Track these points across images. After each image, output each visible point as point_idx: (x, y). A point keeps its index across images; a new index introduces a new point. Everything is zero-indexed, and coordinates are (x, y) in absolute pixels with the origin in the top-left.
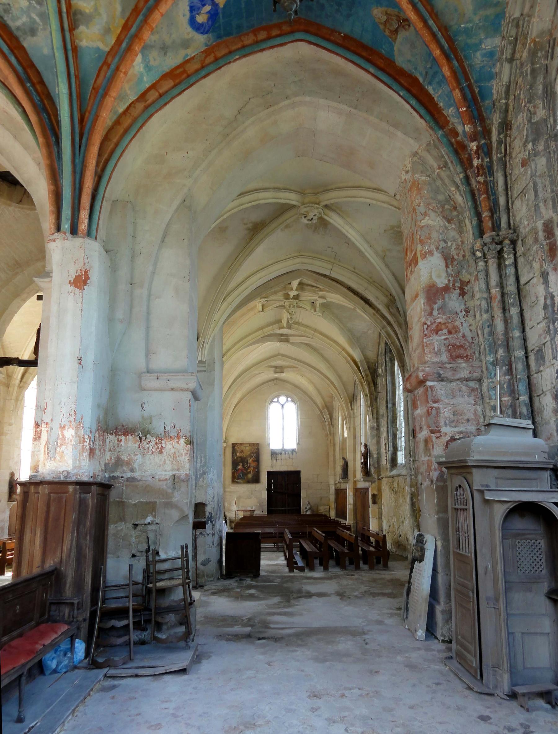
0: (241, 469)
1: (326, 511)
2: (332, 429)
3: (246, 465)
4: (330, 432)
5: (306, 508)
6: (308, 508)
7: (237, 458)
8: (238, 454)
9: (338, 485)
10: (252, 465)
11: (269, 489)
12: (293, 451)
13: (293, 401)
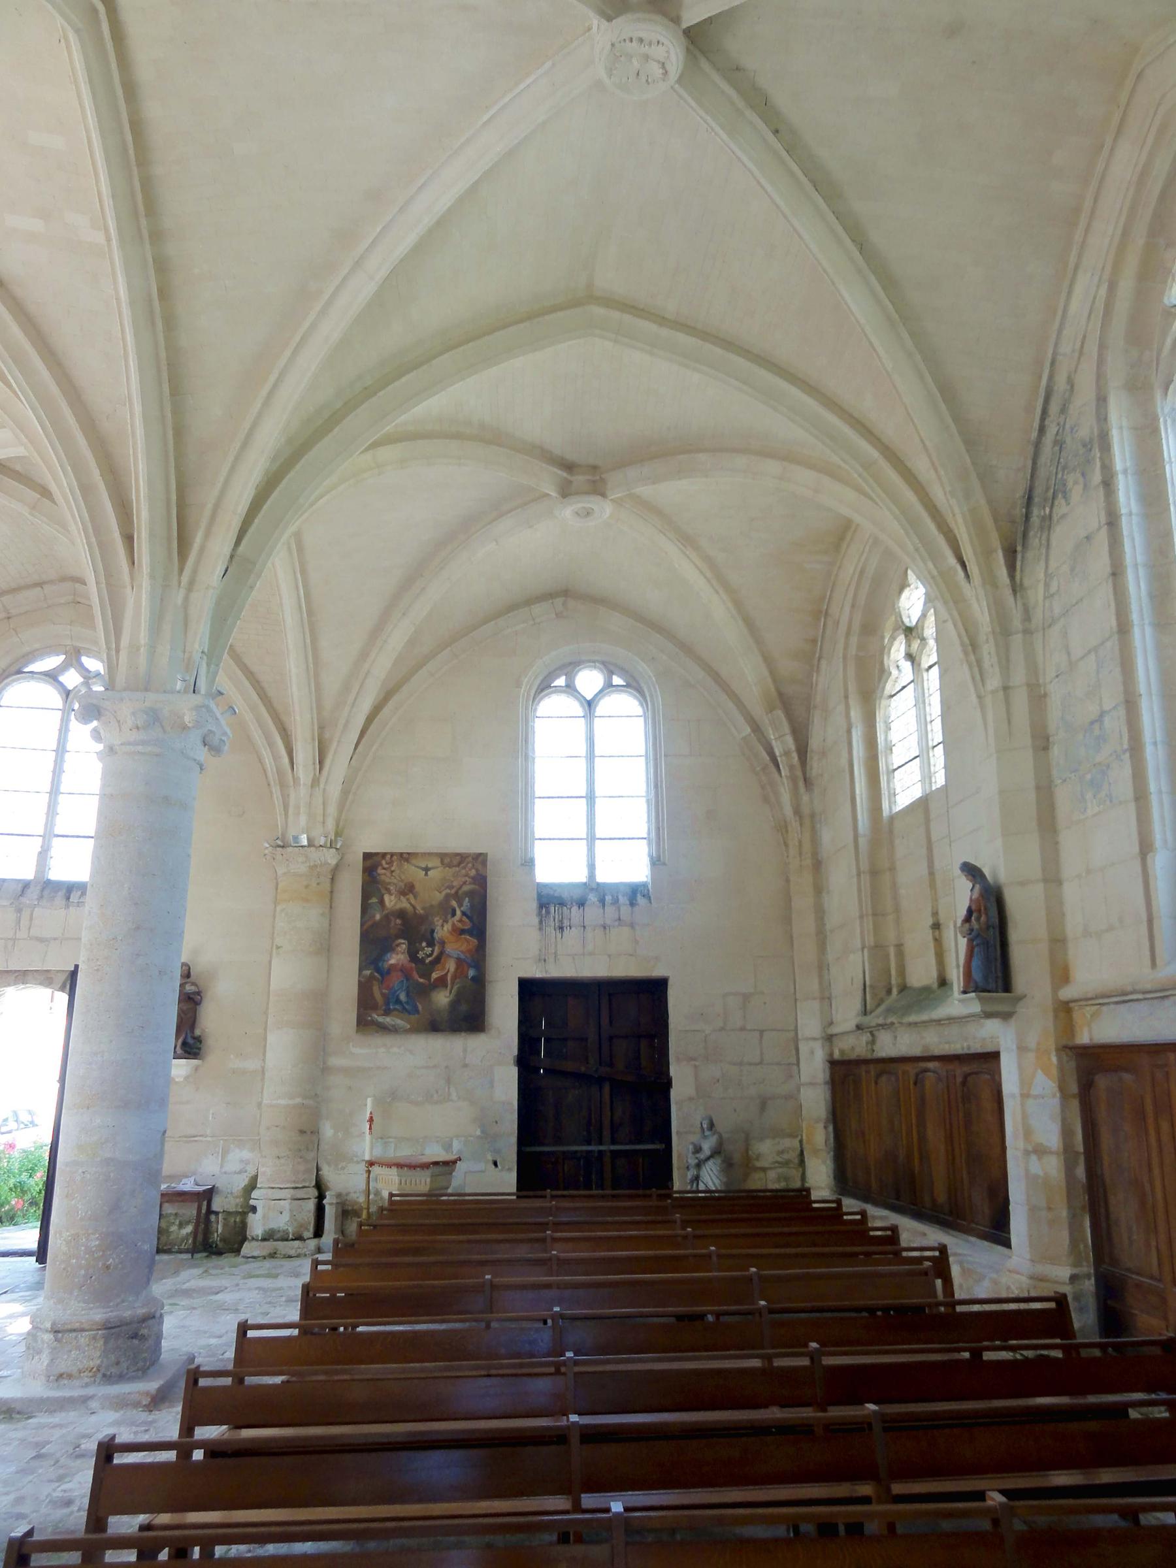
0: (403, 970)
1: (786, 1163)
2: (805, 798)
4: (797, 812)
5: (698, 1150)
6: (707, 1147)
7: (387, 918)
8: (390, 901)
9: (855, 1046)
10: (449, 949)
11: (525, 1061)
12: (635, 892)
13: (634, 685)
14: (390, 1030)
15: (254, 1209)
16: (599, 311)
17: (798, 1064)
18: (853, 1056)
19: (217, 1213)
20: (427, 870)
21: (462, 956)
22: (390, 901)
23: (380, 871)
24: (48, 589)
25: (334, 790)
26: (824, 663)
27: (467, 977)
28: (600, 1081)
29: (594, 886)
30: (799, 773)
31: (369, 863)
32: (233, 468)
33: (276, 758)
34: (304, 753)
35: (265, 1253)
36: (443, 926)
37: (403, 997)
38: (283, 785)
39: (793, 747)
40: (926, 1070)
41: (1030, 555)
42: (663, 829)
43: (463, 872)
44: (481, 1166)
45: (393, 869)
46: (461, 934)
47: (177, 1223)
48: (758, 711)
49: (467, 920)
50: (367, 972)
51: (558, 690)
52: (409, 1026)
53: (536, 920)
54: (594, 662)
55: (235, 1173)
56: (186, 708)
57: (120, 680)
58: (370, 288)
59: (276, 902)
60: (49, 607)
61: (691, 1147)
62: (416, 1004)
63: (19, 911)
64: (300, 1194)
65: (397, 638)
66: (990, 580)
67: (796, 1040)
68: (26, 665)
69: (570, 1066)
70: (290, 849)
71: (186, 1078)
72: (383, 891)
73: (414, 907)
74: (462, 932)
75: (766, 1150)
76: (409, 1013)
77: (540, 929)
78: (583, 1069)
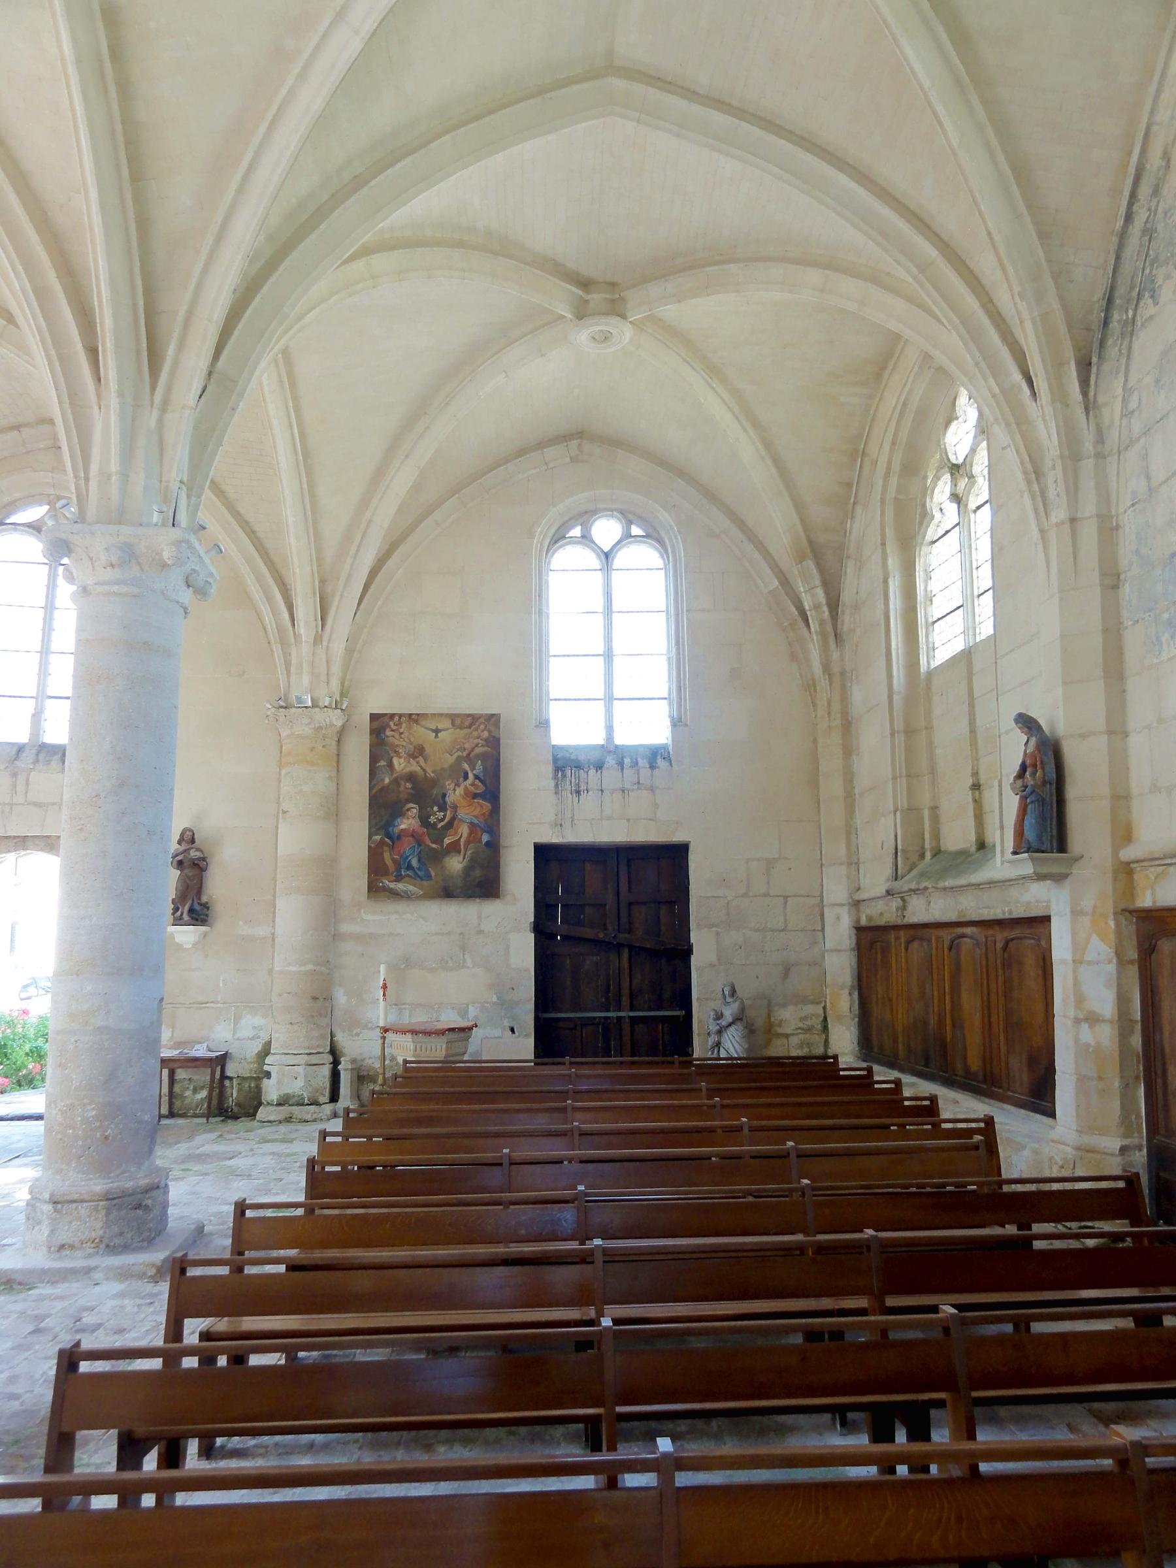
1: (809, 1030)
2: (835, 655)
3: (436, 815)
4: (826, 669)
5: (719, 1016)
6: (729, 1014)
7: (396, 781)
8: (399, 764)
9: (885, 912)
10: (462, 813)
11: (542, 931)
12: (655, 755)
13: (653, 536)
14: (402, 897)
15: (268, 1075)
16: (619, 84)
17: (823, 930)
18: (882, 922)
19: (231, 1079)
20: (437, 731)
21: (476, 821)
22: (399, 764)
23: (388, 733)
24: (26, 432)
25: (338, 648)
26: (859, 509)
27: (480, 842)
28: (619, 946)
29: (612, 748)
30: (829, 628)
31: (376, 725)
32: (205, 270)
33: (275, 612)
34: (305, 610)
35: (281, 1117)
36: (454, 790)
37: (415, 863)
38: (284, 643)
39: (824, 601)
40: (963, 936)
41: (1106, 367)
42: (685, 689)
43: (475, 734)
44: (497, 1032)
45: (401, 730)
46: (474, 798)
47: (192, 1088)
48: (785, 560)
49: (480, 784)
50: (378, 838)
51: (574, 541)
52: (421, 893)
53: (552, 783)
54: (612, 510)
55: (248, 1038)
56: (164, 542)
57: (91, 511)
58: (356, 45)
59: (280, 766)
60: (28, 452)
61: (712, 1013)
62: (428, 870)
63: (15, 775)
64: (314, 1059)
65: (402, 480)
66: (1060, 396)
67: (821, 906)
68: (8, 516)
69: (587, 932)
70: (293, 710)
71: (195, 945)
72: (392, 754)
73: (424, 770)
74: (475, 796)
75: (789, 1017)
76: (422, 879)
77: (556, 793)
78: (601, 935)
